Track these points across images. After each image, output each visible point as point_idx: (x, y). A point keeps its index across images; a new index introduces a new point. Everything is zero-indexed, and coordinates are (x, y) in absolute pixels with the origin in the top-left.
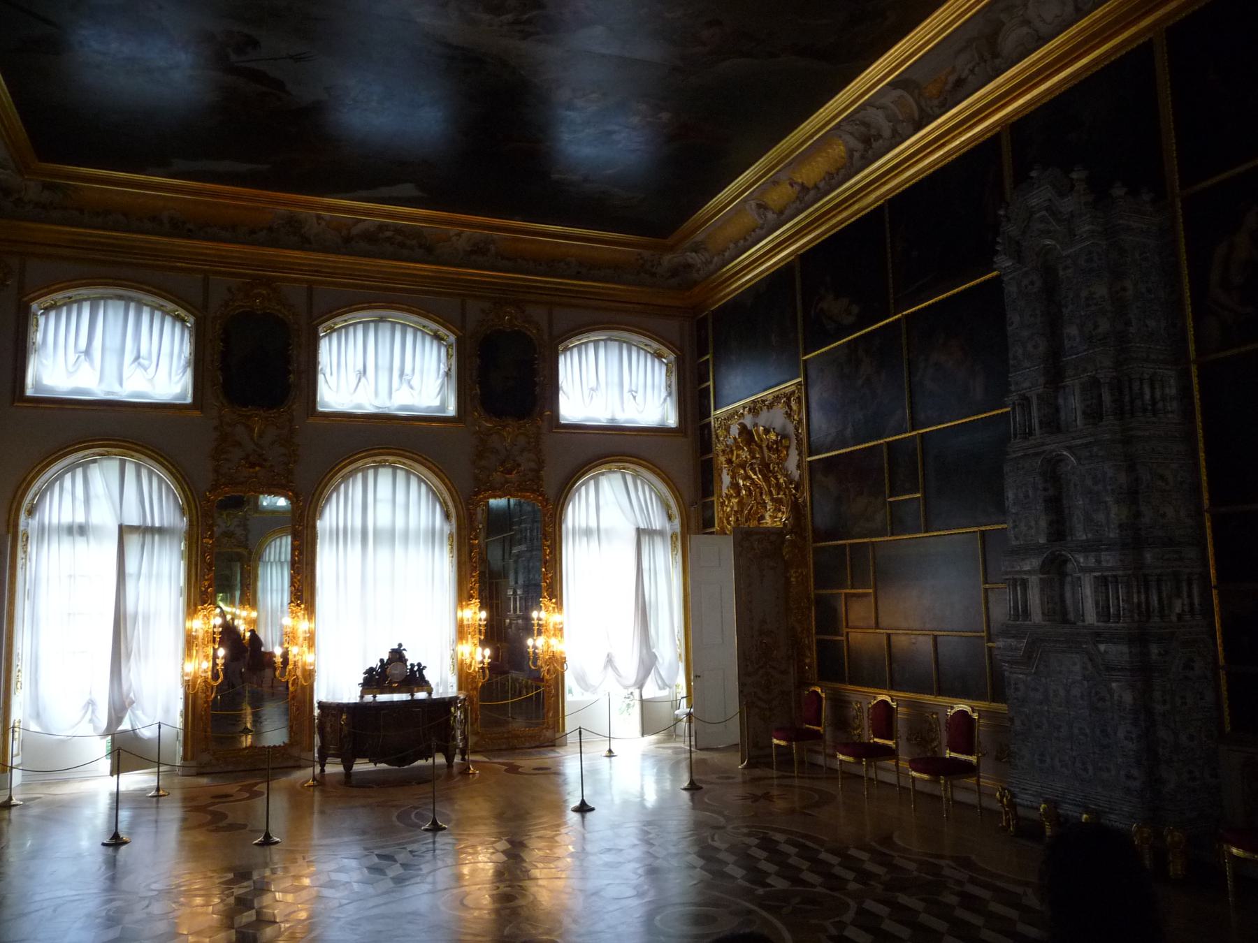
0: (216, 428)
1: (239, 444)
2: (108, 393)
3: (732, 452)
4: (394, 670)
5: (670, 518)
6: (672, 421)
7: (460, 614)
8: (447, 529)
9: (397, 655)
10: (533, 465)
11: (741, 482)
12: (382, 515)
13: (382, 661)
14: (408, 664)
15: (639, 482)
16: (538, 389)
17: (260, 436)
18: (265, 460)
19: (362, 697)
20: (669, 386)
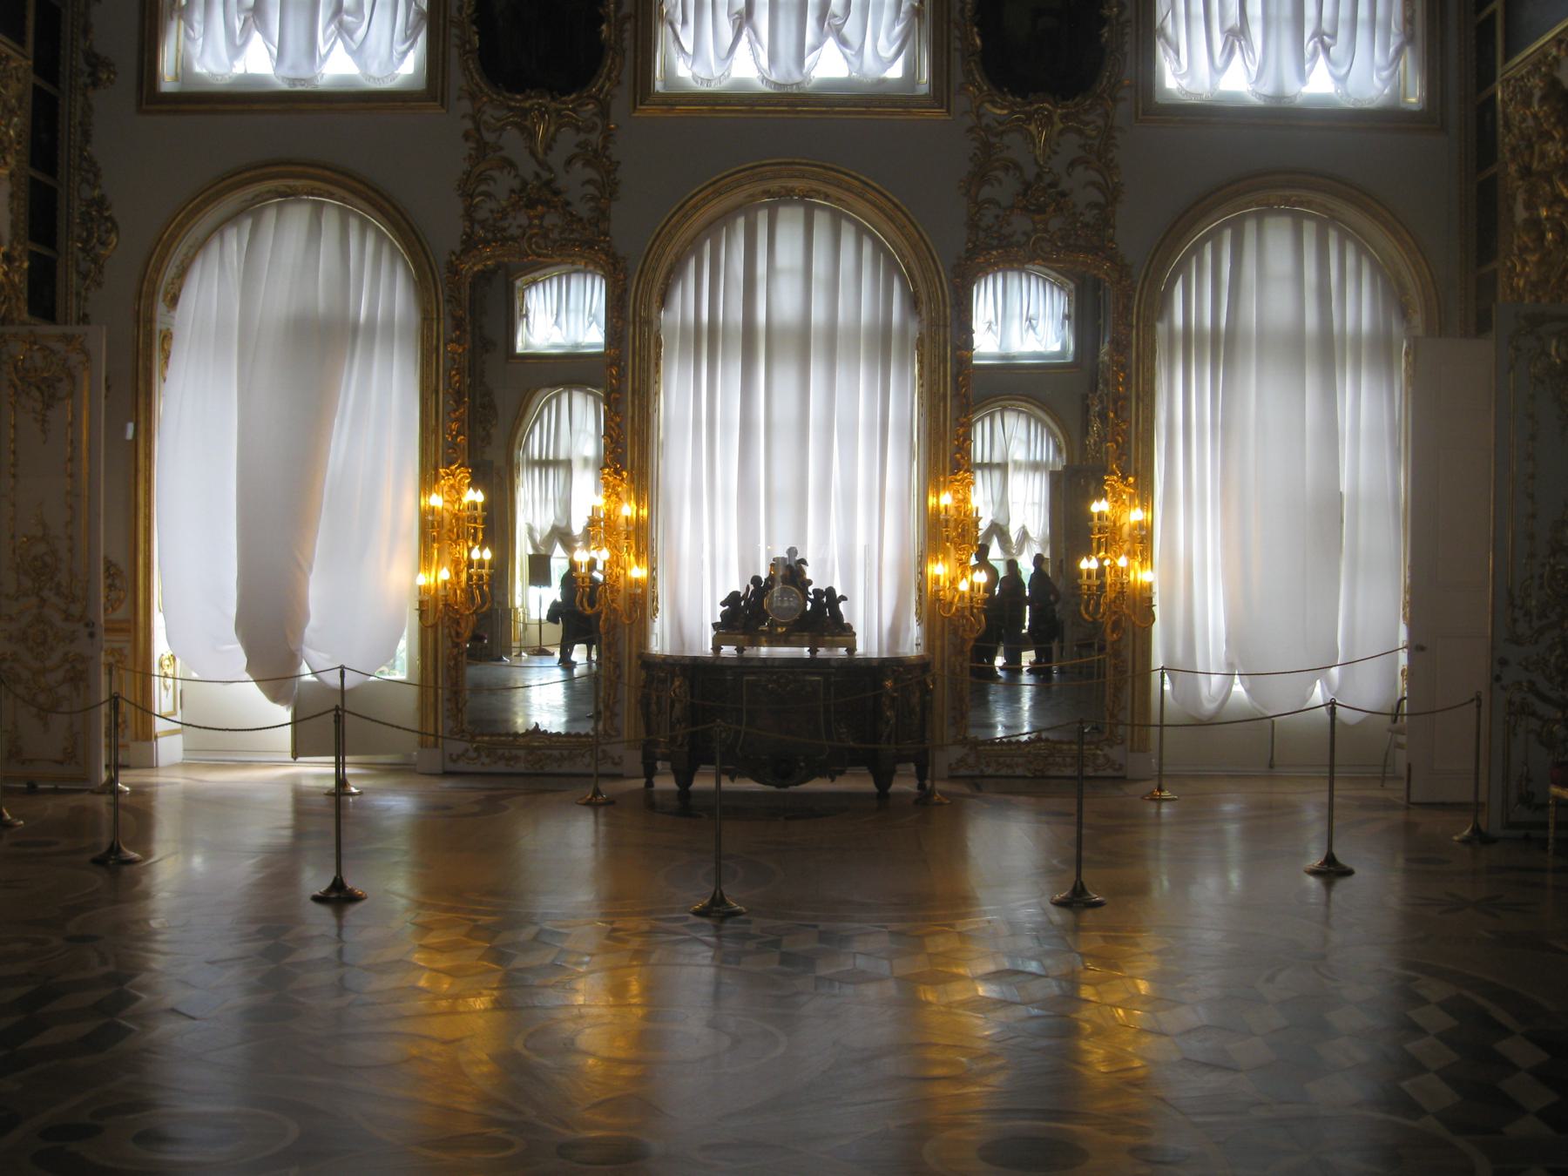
0: (466, 136)
1: (508, 164)
2: (294, 81)
3: (1530, 146)
4: (777, 598)
5: (1405, 314)
6: (1414, 98)
7: (932, 501)
8: (914, 329)
9: (791, 572)
10: (1095, 195)
11: (1544, 213)
12: (783, 300)
13: (756, 580)
14: (810, 589)
15: (1333, 237)
16: (1105, 32)
17: (548, 148)
18: (556, 193)
19: (716, 648)
20: (1408, 21)
